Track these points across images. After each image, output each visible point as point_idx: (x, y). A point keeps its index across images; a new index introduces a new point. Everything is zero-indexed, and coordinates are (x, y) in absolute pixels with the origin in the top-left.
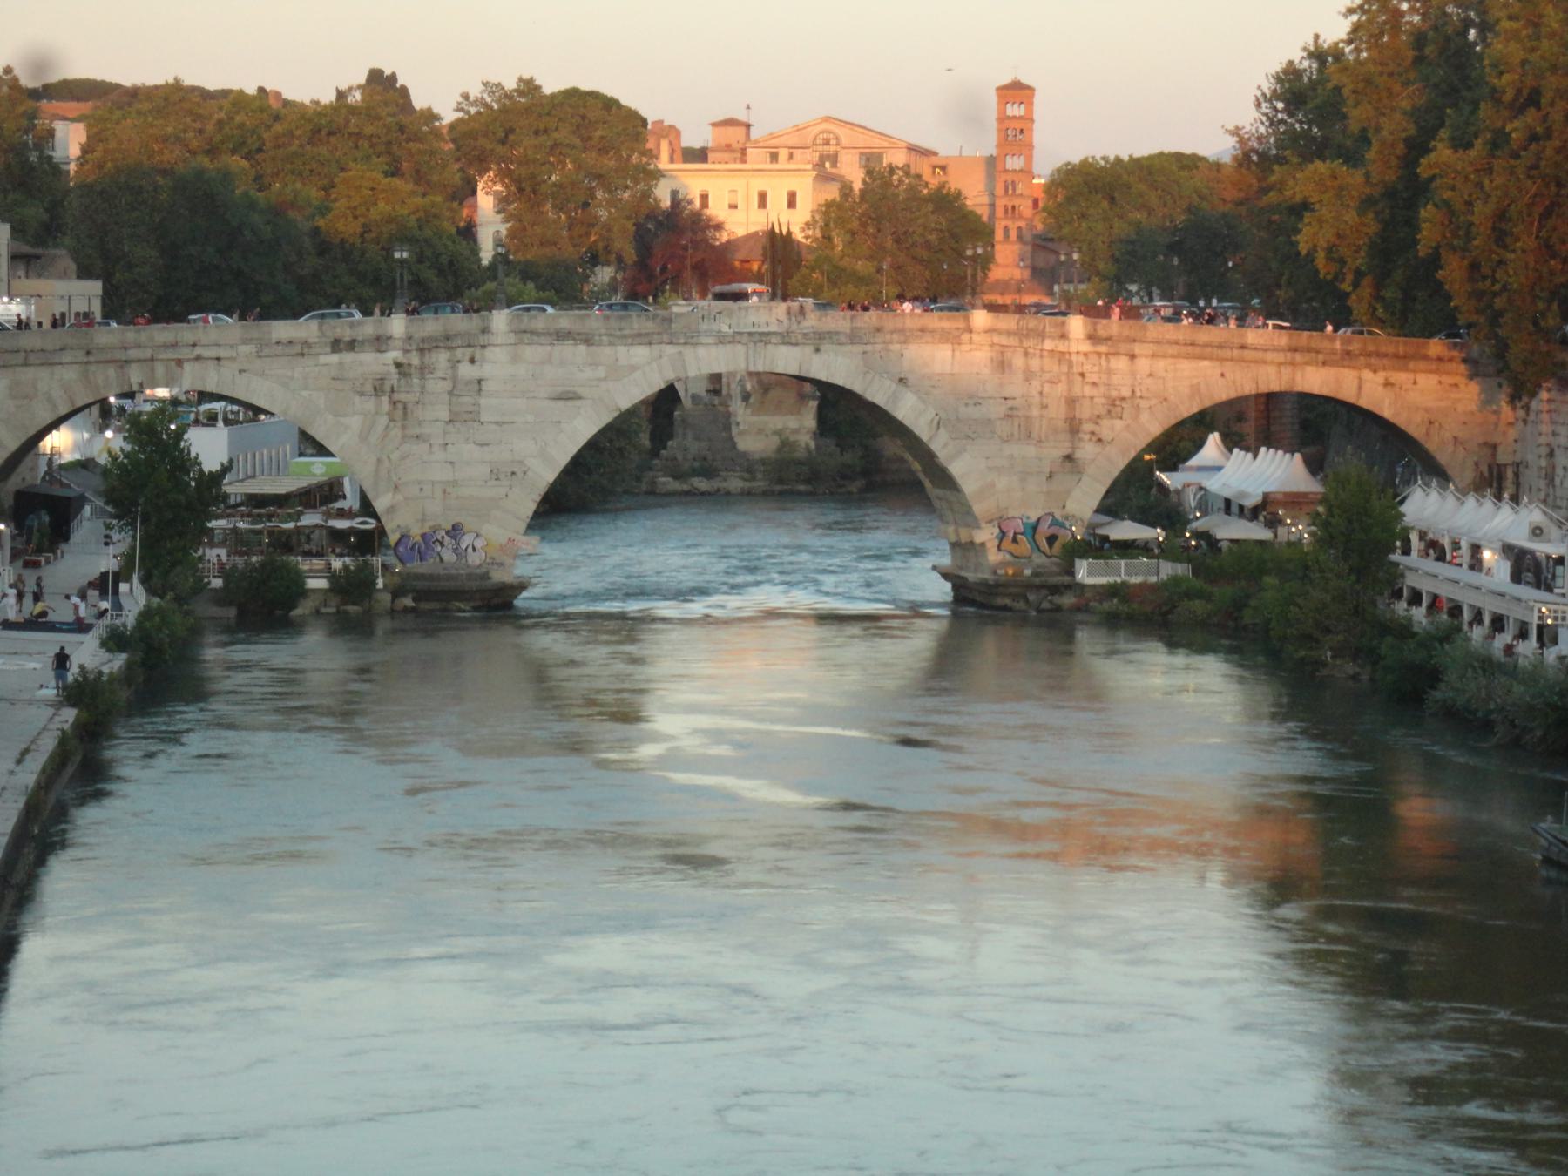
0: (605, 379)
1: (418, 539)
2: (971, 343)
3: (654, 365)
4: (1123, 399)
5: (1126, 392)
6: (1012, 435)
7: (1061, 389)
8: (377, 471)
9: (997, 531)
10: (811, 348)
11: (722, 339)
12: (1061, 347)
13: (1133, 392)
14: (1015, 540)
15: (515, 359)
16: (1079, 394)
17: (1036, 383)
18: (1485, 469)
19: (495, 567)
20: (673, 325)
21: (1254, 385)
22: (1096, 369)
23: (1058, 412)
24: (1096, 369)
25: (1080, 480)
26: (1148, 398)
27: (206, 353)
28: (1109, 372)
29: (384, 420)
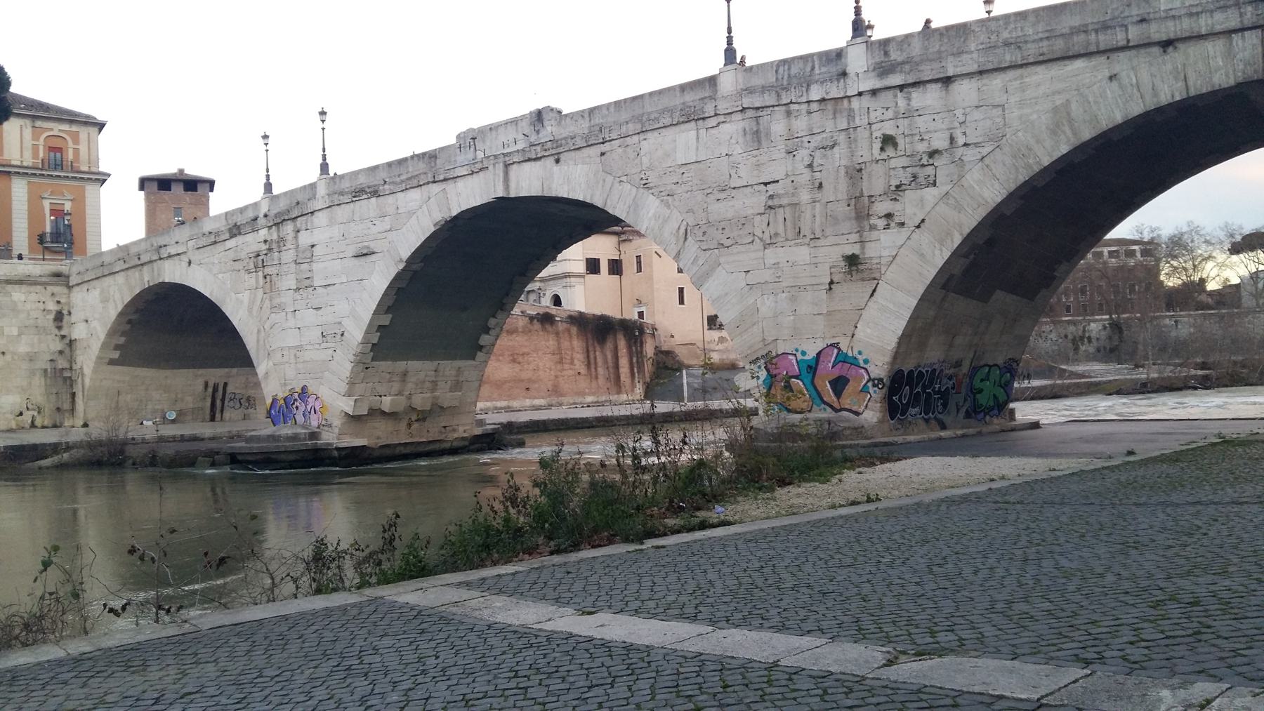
0: (390, 230)
1: (282, 402)
2: (716, 115)
3: (425, 207)
4: (933, 154)
5: (940, 142)
6: (776, 234)
7: (839, 156)
8: (258, 341)
9: (763, 374)
10: (551, 161)
11: (477, 169)
12: (835, 92)
13: (952, 139)
14: (788, 387)
15: (332, 222)
16: (867, 158)
17: (803, 154)
19: (326, 428)
20: (438, 161)
21: (1181, 84)
22: (890, 114)
23: (837, 189)
24: (890, 114)
25: (874, 291)
26: (976, 145)
27: (173, 251)
28: (909, 114)
29: (260, 292)
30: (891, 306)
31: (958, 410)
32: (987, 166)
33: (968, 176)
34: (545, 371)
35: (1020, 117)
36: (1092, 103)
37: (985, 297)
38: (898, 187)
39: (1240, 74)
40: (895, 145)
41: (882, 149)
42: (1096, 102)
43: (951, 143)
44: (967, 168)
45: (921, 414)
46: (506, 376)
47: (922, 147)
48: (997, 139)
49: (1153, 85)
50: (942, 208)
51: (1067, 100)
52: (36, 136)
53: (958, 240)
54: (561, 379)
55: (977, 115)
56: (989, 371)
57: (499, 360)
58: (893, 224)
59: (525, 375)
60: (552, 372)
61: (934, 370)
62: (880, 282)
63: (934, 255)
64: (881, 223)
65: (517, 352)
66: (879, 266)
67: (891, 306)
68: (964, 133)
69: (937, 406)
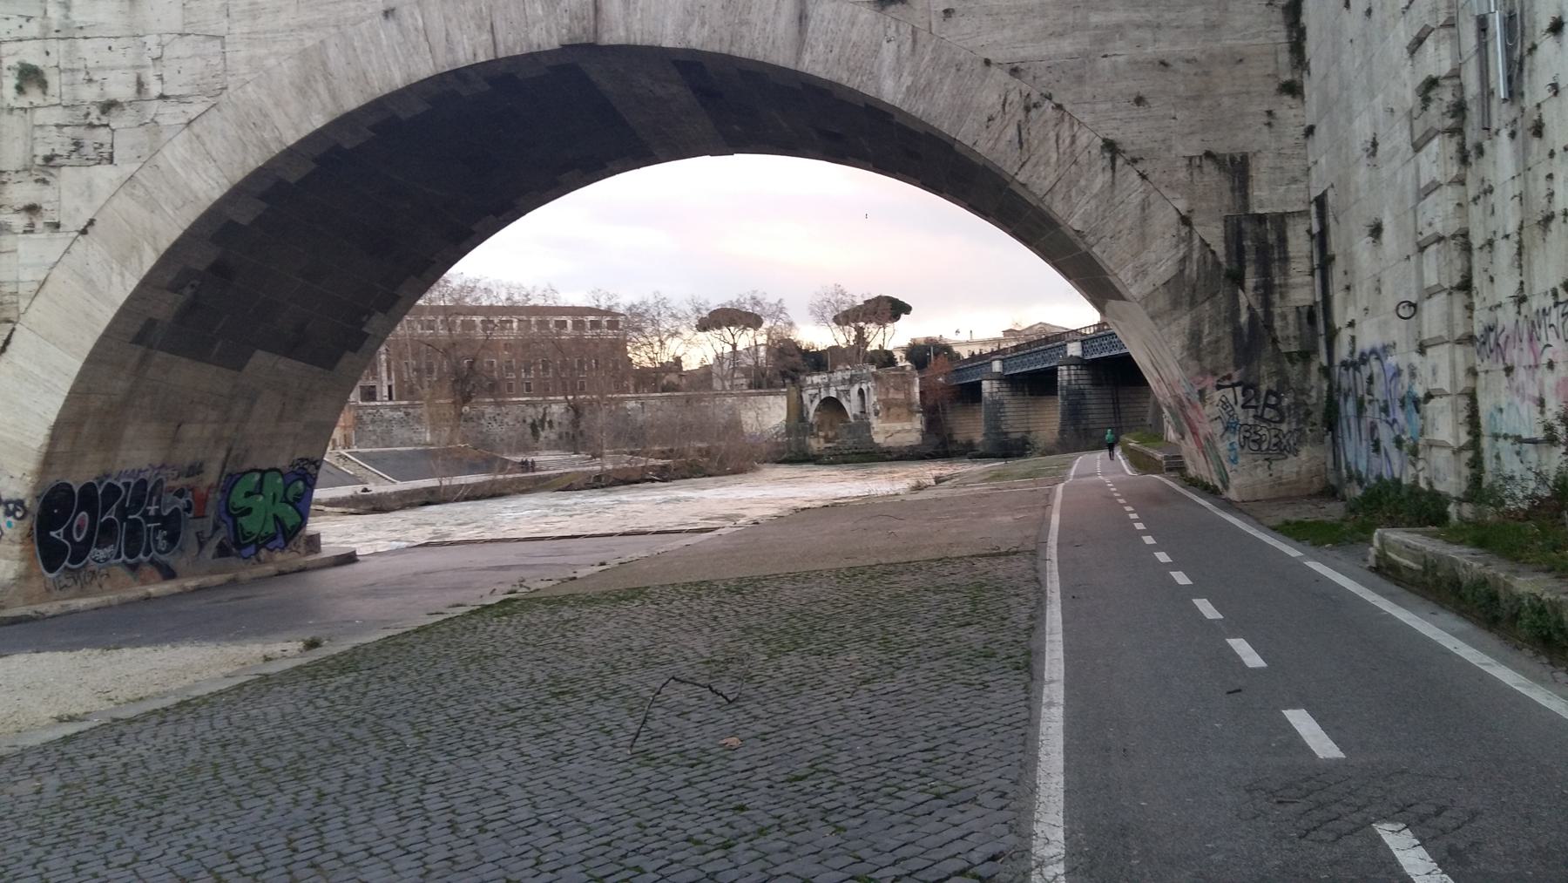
4: (108, 106)
5: (121, 89)
13: (140, 85)
18: (1213, 233)
21: (486, 37)
22: (33, 29)
24: (33, 29)
26: (180, 99)
30: (37, 370)
31: (201, 545)
32: (198, 137)
33: (166, 151)
35: (249, 61)
36: (359, 51)
37: (236, 361)
38: (48, 159)
39: (564, 31)
40: (43, 85)
41: (20, 89)
42: (366, 51)
43: (139, 91)
44: (166, 135)
45: (118, 556)
47: (89, 94)
48: (215, 93)
49: (448, 34)
50: (124, 203)
51: (322, 42)
53: (149, 260)
55: (180, 48)
56: (261, 481)
58: (39, 225)
61: (143, 483)
62: (18, 327)
63: (110, 283)
64: (19, 221)
66: (14, 298)
67: (37, 370)
68: (161, 78)
69: (156, 542)
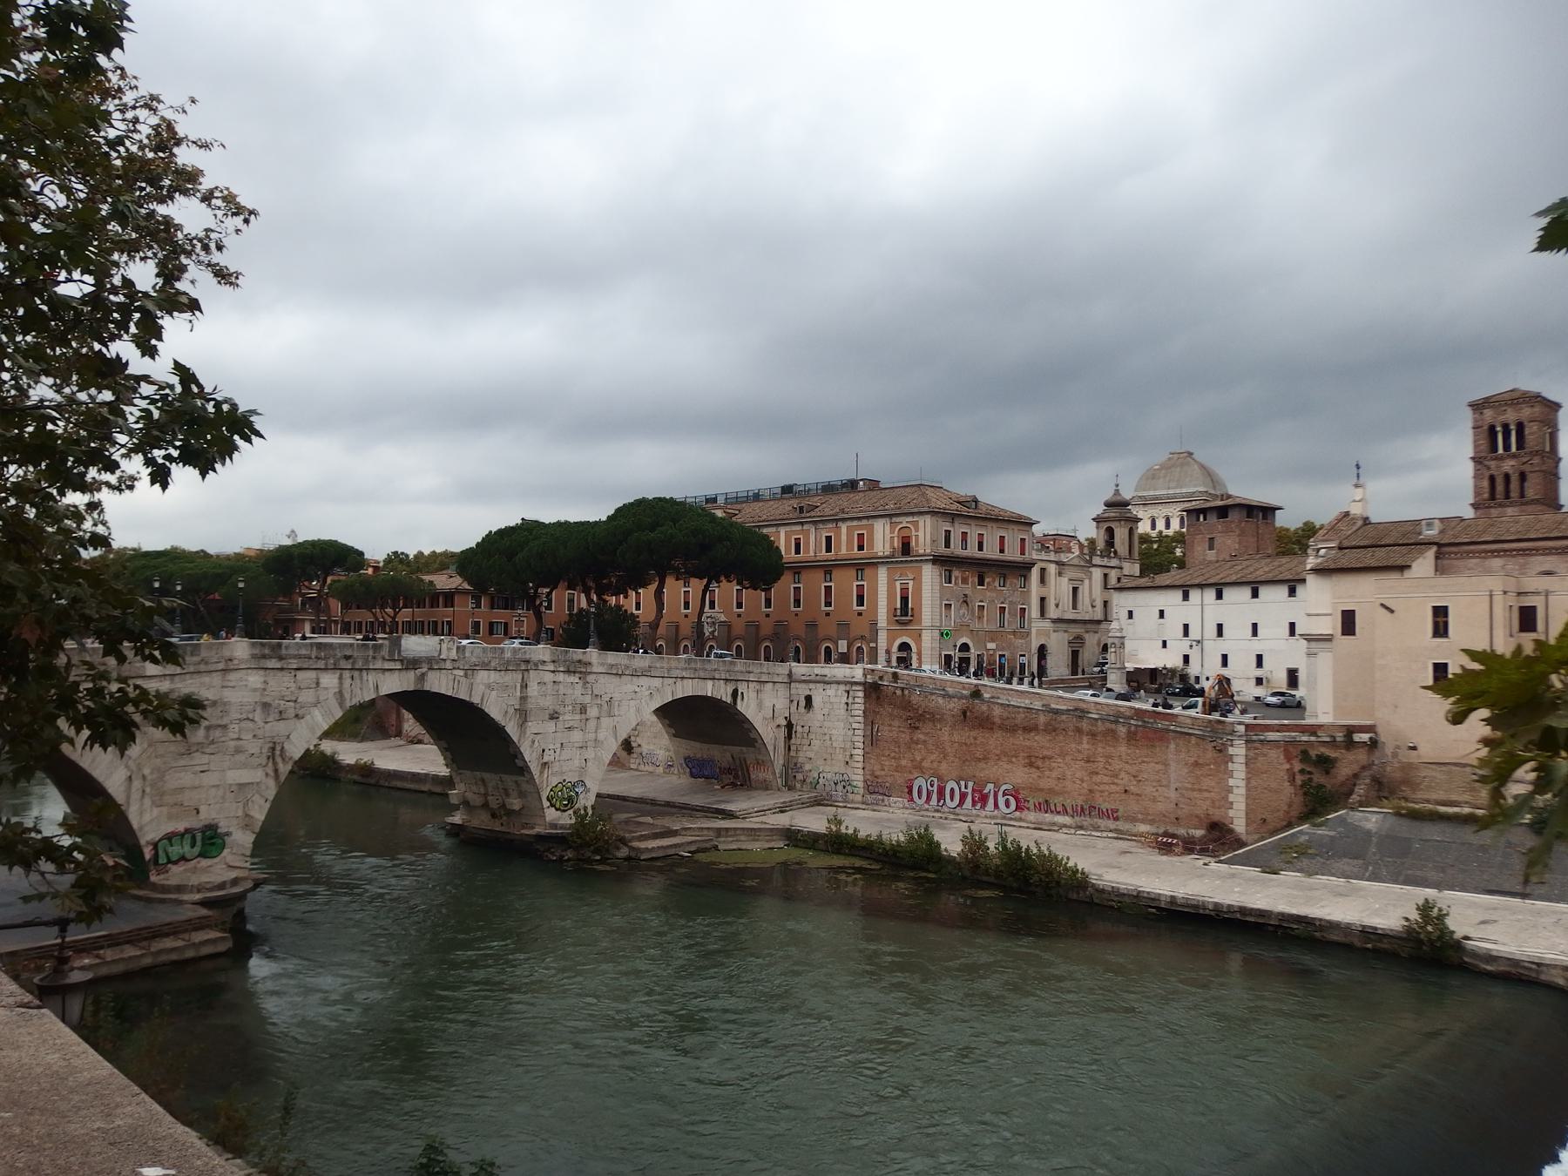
34: (1074, 782)
46: (1020, 781)
52: (892, 532)
54: (1098, 794)
57: (1012, 762)
59: (1044, 784)
60: (1085, 785)
65: (1037, 754)
